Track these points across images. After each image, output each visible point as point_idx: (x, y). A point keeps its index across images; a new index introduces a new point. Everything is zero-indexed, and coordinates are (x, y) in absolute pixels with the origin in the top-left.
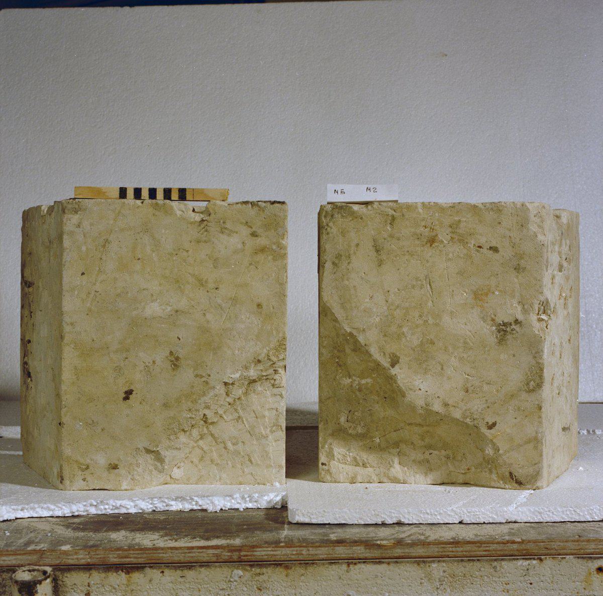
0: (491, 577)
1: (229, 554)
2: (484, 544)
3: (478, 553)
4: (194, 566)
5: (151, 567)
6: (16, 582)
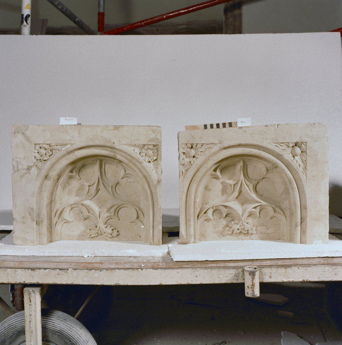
1: (324, 261)
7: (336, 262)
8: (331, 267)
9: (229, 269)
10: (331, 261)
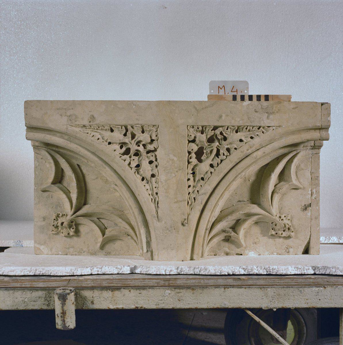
0: (299, 296)
1: (164, 282)
2: (295, 279)
3: (292, 283)
4: (146, 288)
5: (124, 288)
6: (57, 294)
7: (180, 284)
8: (173, 291)
9: (37, 290)
10: (173, 282)
